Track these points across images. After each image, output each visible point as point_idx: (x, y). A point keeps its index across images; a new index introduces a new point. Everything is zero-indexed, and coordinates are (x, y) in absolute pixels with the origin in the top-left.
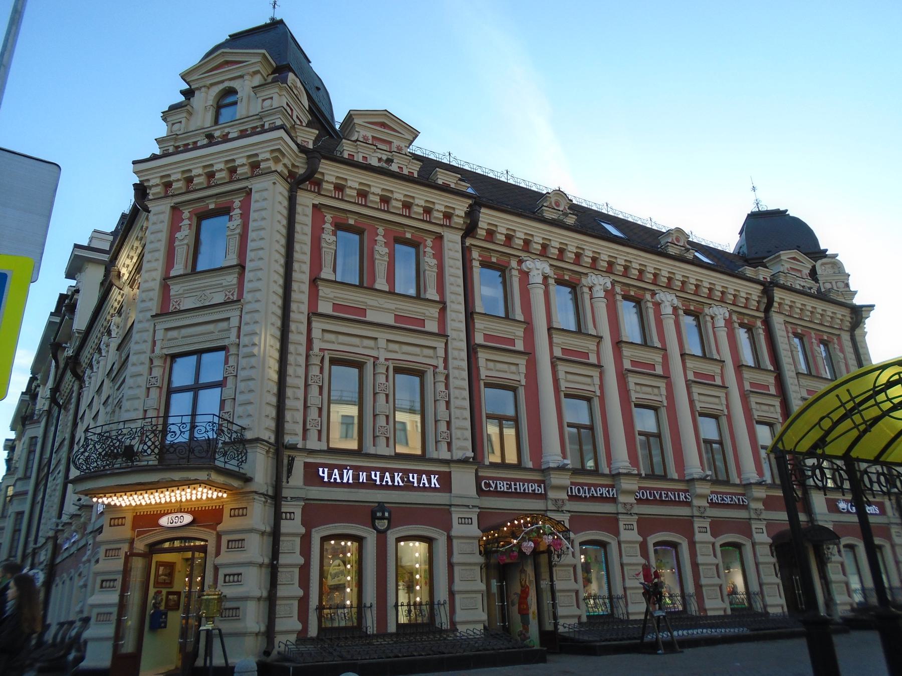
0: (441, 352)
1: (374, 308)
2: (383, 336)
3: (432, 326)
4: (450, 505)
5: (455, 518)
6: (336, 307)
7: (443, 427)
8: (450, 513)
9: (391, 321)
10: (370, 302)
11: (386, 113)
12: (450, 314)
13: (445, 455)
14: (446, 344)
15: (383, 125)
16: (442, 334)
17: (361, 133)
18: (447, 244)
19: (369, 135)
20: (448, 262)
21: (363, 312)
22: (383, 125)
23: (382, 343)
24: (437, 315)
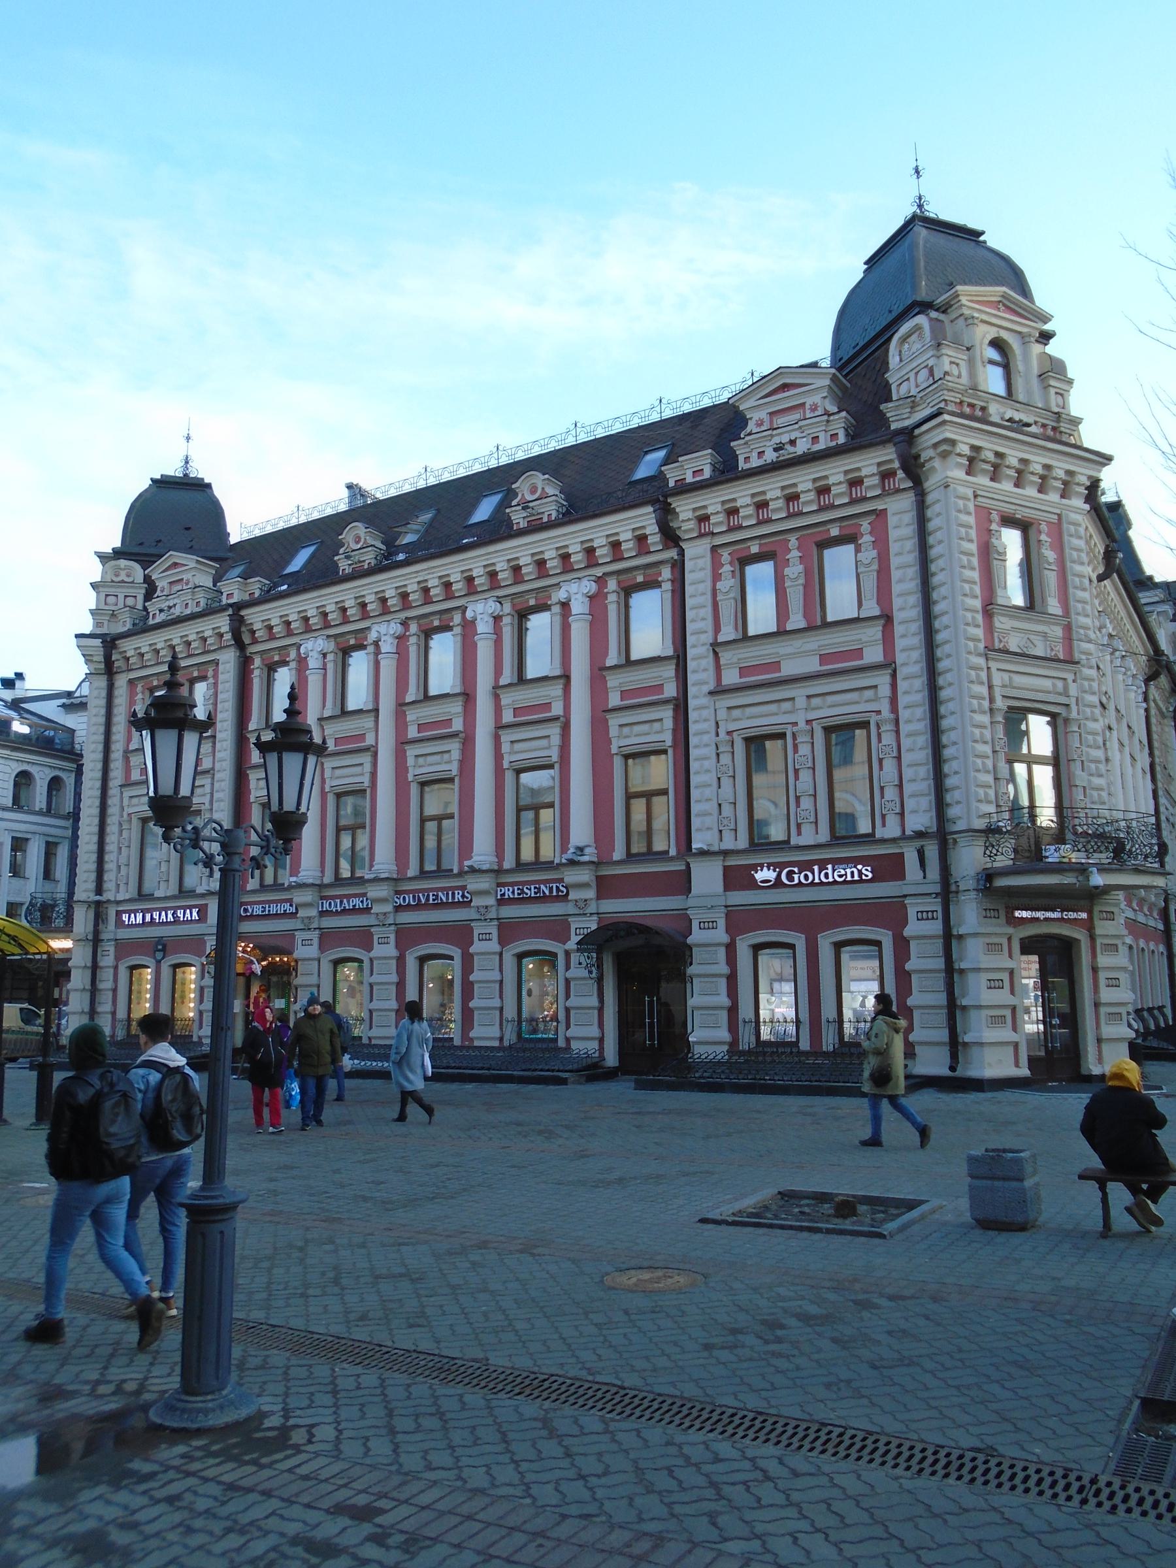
0: (885, 691)
1: (791, 656)
2: (799, 692)
3: (874, 655)
4: (905, 896)
5: (912, 913)
6: (743, 671)
7: (891, 793)
8: (905, 907)
9: (813, 665)
10: (782, 651)
11: (780, 371)
12: (899, 629)
13: (891, 830)
14: (894, 675)
15: (785, 387)
16: (889, 665)
17: (756, 416)
18: (892, 520)
19: (763, 414)
20: (894, 548)
21: (776, 666)
22: (785, 387)
23: (801, 702)
24: (879, 635)
